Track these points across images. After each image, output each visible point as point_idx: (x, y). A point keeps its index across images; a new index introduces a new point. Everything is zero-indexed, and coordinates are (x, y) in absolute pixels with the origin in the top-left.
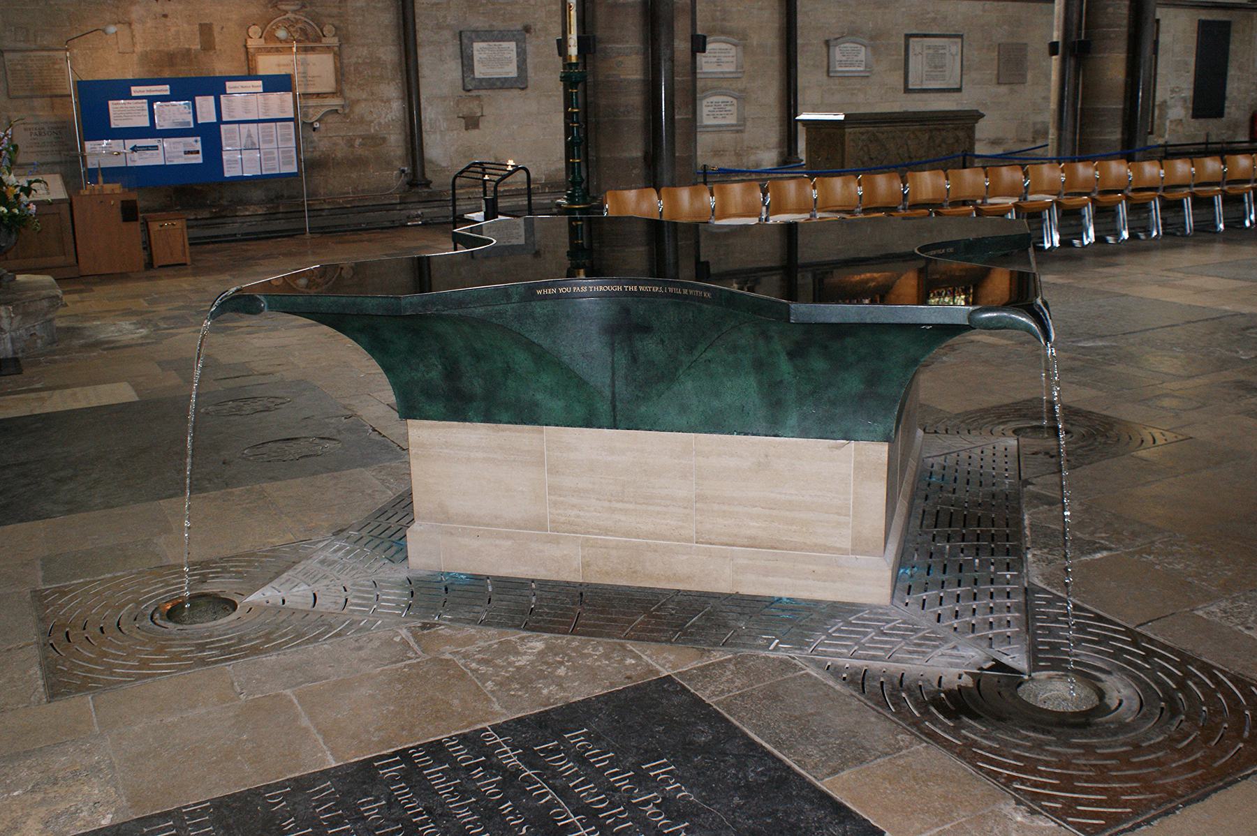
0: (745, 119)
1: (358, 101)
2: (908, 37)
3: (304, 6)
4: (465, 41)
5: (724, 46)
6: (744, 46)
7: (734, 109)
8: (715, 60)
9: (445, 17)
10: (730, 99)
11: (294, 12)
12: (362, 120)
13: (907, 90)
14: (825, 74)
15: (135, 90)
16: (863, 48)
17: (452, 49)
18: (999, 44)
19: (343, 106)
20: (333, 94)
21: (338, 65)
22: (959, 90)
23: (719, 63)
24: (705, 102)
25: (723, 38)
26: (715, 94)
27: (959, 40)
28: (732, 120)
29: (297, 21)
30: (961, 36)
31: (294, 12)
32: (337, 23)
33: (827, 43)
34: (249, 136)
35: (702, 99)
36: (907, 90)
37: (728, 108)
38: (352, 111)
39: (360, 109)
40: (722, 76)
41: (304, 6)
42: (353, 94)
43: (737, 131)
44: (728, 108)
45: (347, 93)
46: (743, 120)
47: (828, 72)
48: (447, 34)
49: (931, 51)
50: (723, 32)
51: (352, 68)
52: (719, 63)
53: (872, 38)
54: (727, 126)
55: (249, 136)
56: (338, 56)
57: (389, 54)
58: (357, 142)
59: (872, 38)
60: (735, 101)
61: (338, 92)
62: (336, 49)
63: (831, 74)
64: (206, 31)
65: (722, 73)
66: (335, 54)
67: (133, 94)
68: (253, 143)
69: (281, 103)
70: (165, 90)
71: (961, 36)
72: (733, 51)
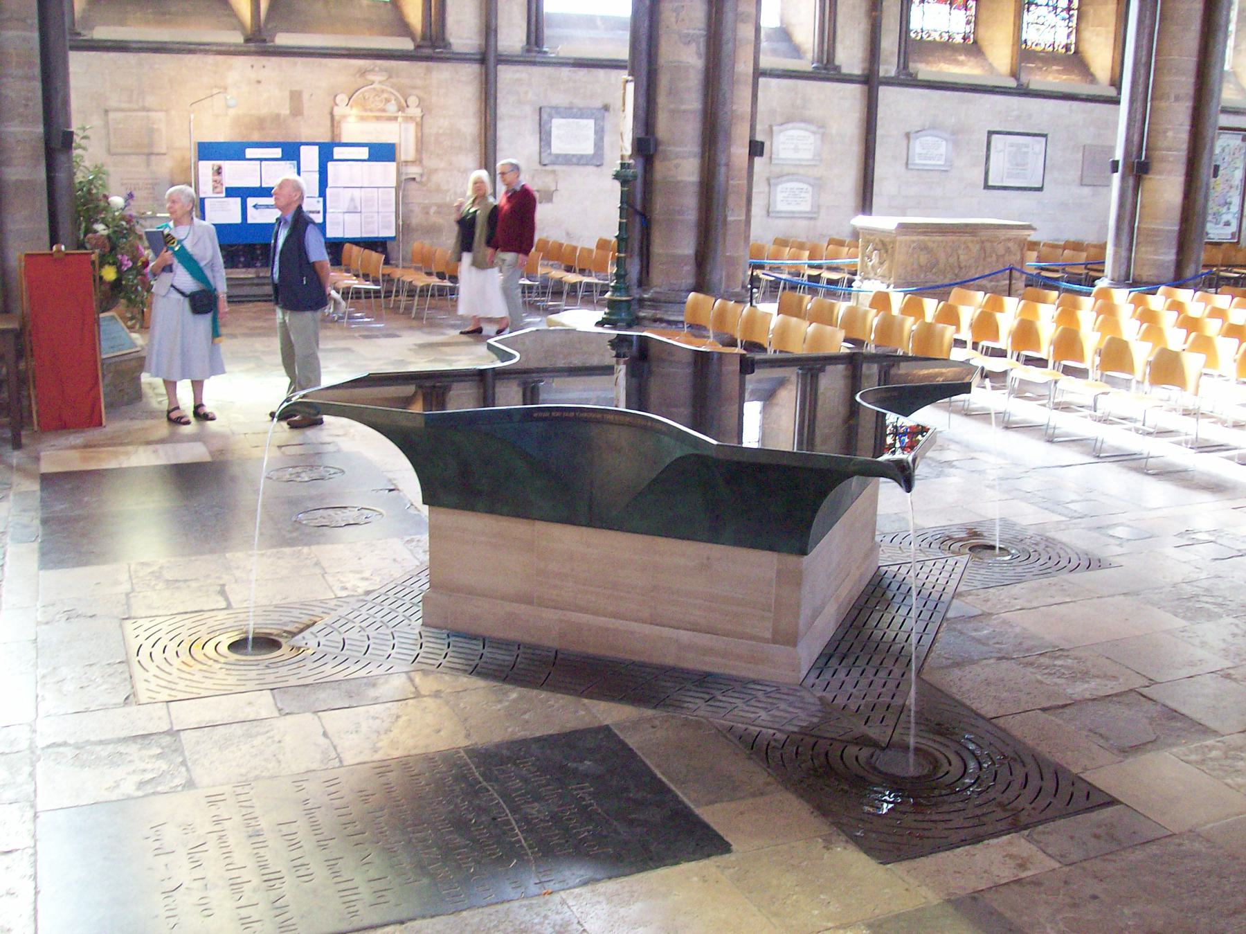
0: (819, 207)
1: (436, 170)
2: (990, 133)
3: (390, 77)
4: (545, 117)
5: (802, 133)
6: (823, 135)
7: (808, 196)
8: (792, 146)
9: (526, 92)
10: (805, 186)
11: (380, 82)
12: (438, 190)
13: (987, 187)
14: (904, 168)
15: (250, 153)
16: (944, 142)
17: (530, 125)
18: (1084, 146)
19: (422, 175)
20: (413, 162)
21: (419, 135)
22: (1040, 189)
23: (796, 150)
24: (779, 188)
25: (802, 125)
26: (791, 181)
27: (1043, 140)
28: (805, 207)
29: (383, 91)
30: (1045, 136)
31: (380, 82)
32: (421, 94)
33: (908, 135)
34: (352, 200)
35: (777, 185)
36: (987, 187)
37: (802, 195)
38: (429, 180)
39: (438, 178)
40: (797, 163)
41: (390, 77)
42: (430, 163)
43: (811, 218)
44: (802, 195)
45: (426, 162)
46: (817, 208)
47: (907, 164)
48: (528, 110)
49: (1014, 149)
50: (804, 120)
51: (433, 138)
52: (796, 150)
53: (954, 133)
54: (801, 212)
55: (352, 200)
56: (420, 126)
57: (469, 126)
58: (432, 210)
59: (954, 133)
60: (810, 189)
61: (418, 161)
62: (418, 119)
63: (910, 167)
64: (296, 97)
65: (799, 160)
66: (417, 124)
67: (248, 156)
68: (355, 207)
69: (385, 172)
70: (277, 152)
71: (1045, 136)
72: (812, 138)
